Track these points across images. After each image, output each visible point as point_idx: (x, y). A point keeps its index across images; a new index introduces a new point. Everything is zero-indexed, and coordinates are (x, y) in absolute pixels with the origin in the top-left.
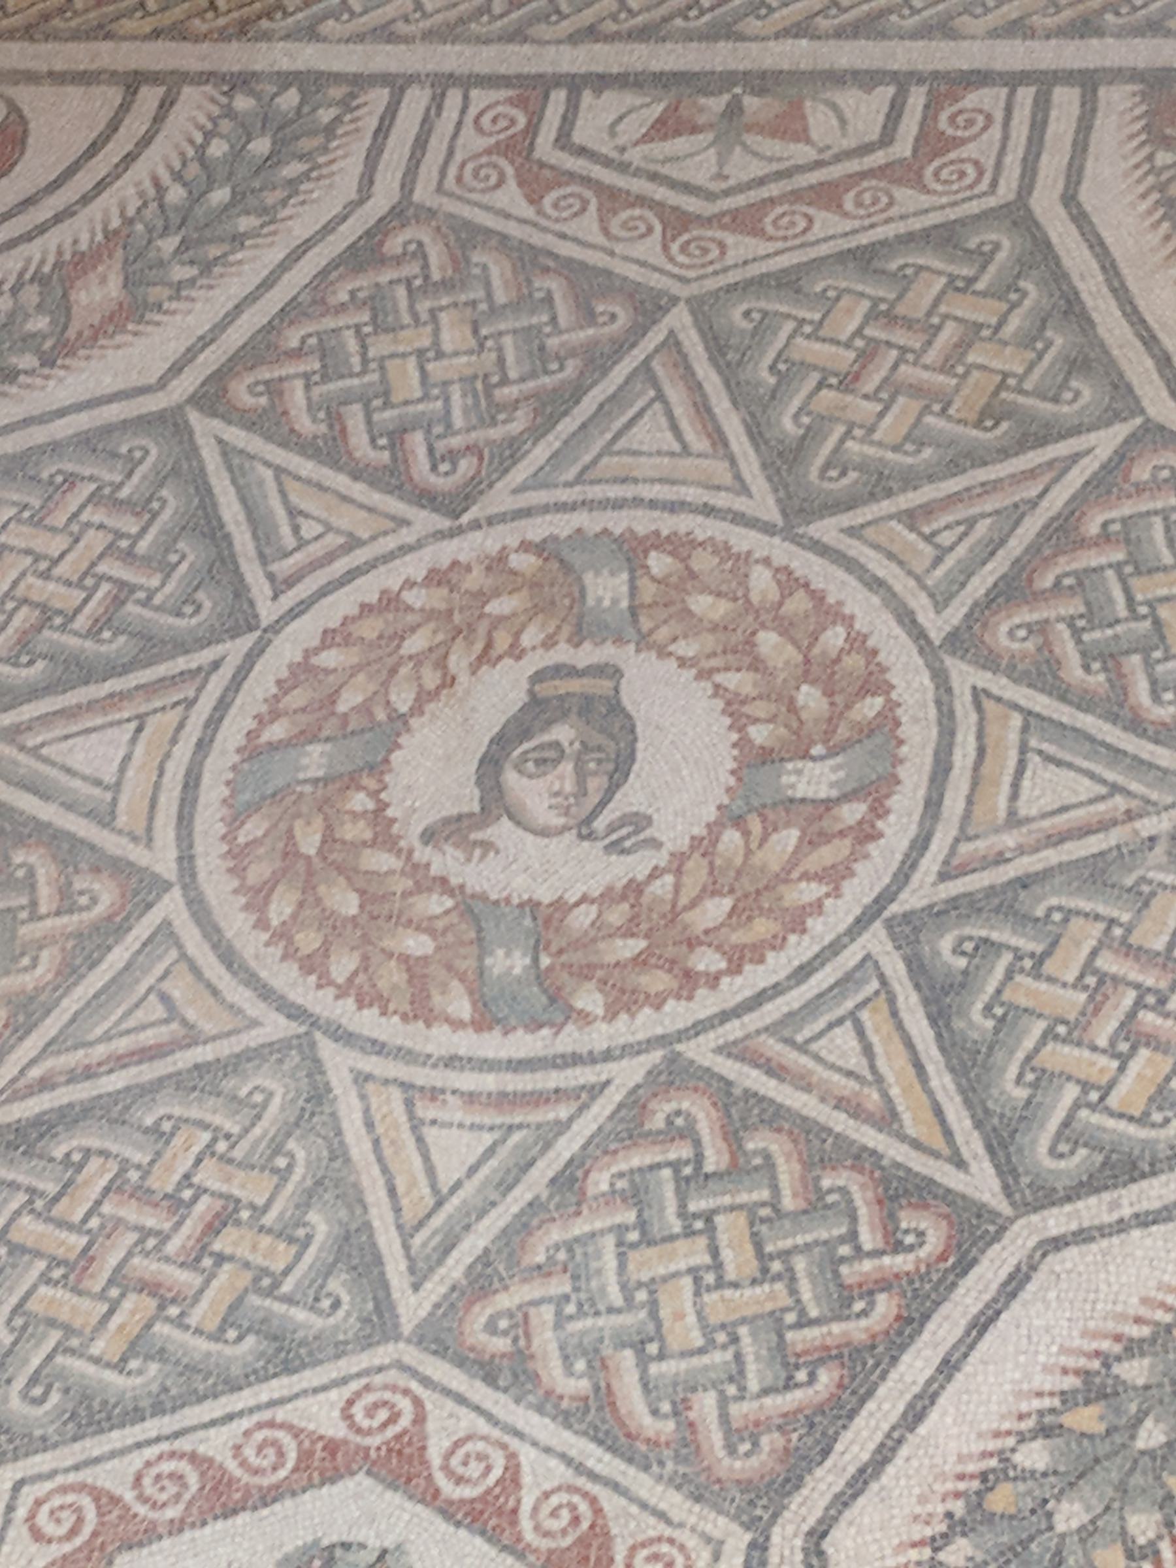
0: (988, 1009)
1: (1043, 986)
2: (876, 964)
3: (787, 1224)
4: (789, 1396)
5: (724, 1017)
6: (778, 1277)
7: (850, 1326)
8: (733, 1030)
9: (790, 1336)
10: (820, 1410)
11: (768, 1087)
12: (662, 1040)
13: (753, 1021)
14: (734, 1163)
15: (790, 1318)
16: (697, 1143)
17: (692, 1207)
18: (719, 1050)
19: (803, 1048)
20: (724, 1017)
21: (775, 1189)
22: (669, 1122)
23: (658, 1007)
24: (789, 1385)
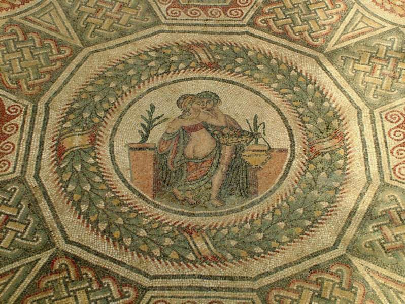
0: (76, 12)
1: (87, 7)
2: (53, 3)
3: (38, 50)
4: (40, 80)
5: (21, 12)
6: (36, 59)
7: (52, 67)
8: (24, 15)
9: (39, 69)
10: (47, 82)
11: (32, 25)
12: (8, 16)
13: (27, 13)
14: (26, 39)
15: (39, 66)
16: (17, 35)
17: (17, 47)
18: (21, 18)
19: (39, 18)
20: (21, 12)
21: (34, 43)
22: (11, 31)
23: (7, 11)
24: (40, 78)
